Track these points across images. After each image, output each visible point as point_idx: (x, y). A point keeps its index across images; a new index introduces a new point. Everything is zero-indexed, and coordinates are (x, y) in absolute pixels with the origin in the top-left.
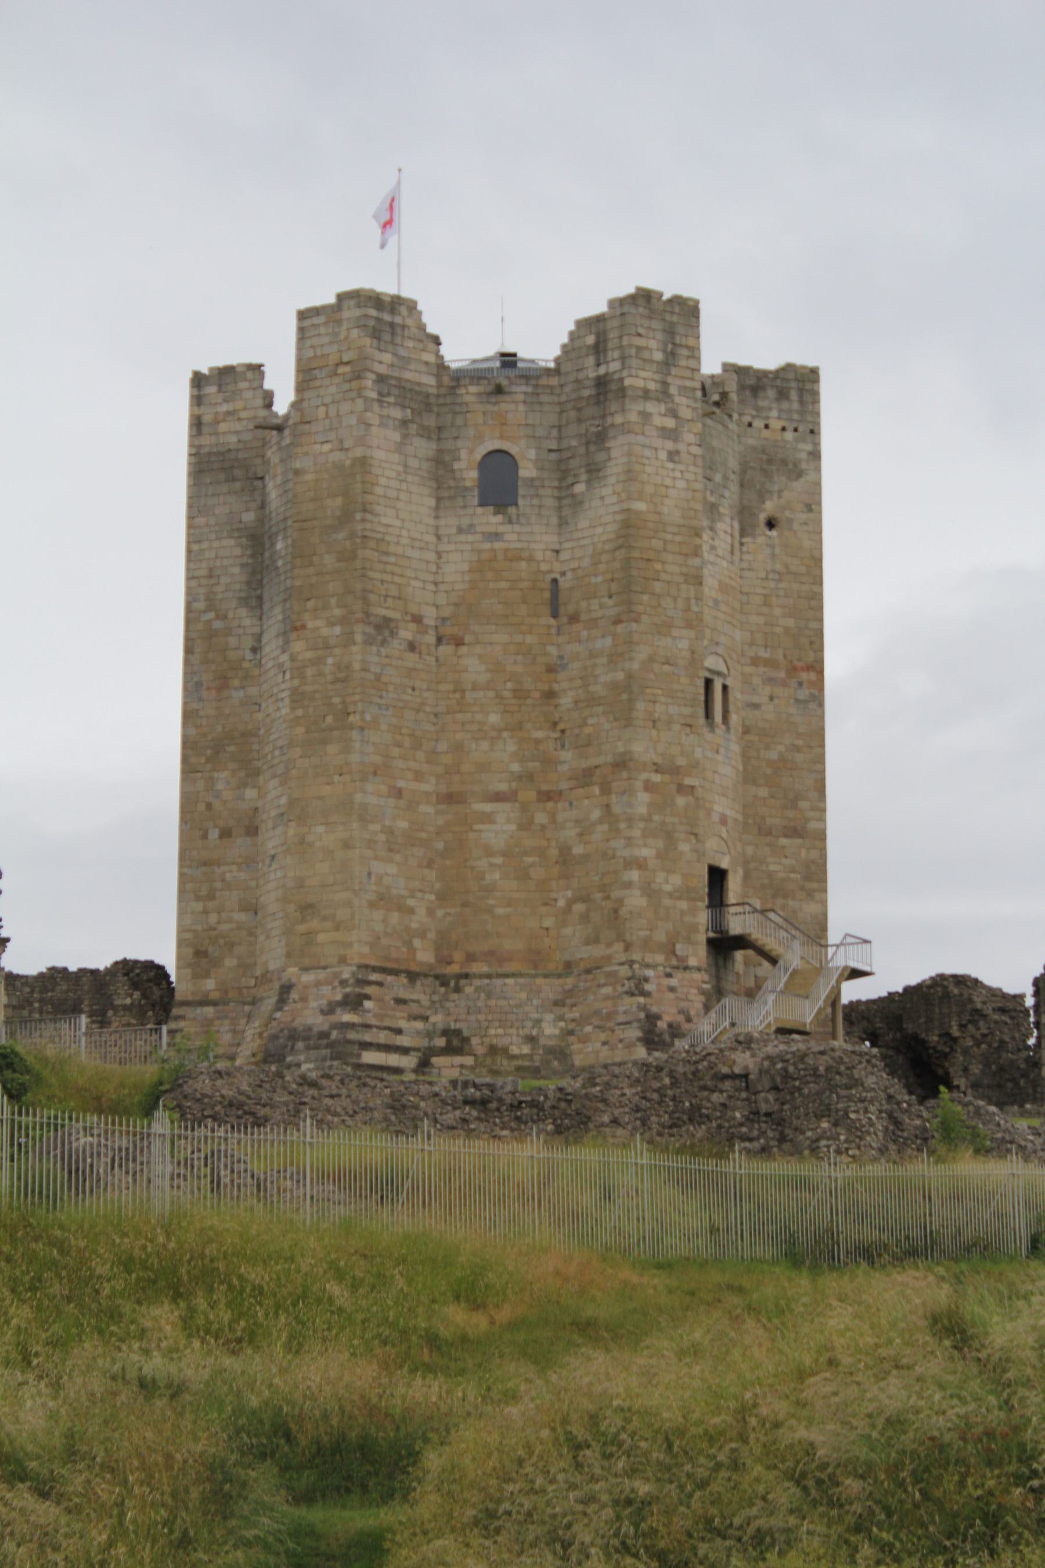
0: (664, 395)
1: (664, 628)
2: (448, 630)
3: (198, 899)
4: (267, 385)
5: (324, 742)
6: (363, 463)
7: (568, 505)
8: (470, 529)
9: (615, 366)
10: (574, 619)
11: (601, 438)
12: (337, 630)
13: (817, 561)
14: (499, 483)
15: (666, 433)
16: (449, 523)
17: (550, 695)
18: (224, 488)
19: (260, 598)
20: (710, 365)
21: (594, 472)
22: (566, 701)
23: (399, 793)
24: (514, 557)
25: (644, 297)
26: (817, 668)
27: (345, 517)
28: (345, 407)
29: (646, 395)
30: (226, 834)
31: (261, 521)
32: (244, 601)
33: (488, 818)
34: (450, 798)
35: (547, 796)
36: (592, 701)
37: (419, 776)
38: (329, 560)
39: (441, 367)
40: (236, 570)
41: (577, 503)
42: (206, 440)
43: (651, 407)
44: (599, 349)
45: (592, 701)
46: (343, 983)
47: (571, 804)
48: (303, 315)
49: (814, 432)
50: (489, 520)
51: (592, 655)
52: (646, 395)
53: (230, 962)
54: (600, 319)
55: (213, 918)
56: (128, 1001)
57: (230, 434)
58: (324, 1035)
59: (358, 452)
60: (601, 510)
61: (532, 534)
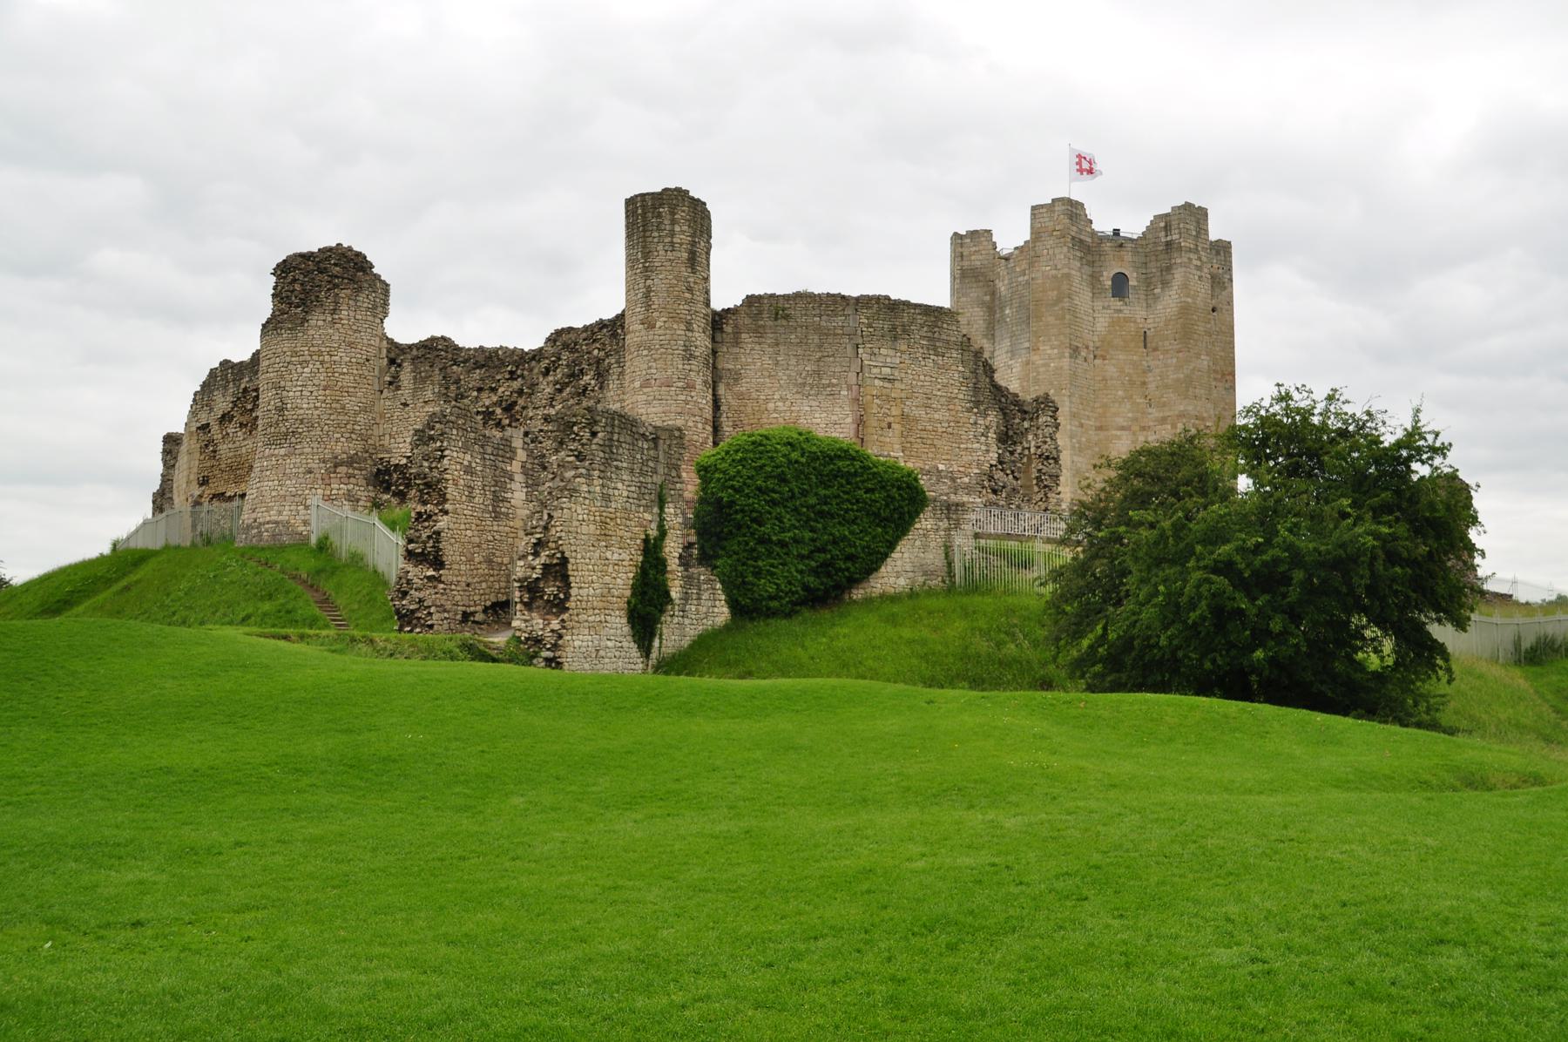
0: (1196, 251)
1: (1198, 356)
2: (1098, 353)
4: (1215, 233)
6: (1068, 276)
7: (1151, 299)
8: (1108, 307)
9: (1175, 237)
10: (1155, 349)
11: (1169, 269)
13: (1232, 328)
14: (1120, 285)
15: (1199, 268)
16: (1099, 304)
17: (1144, 383)
20: (1213, 235)
21: (1165, 284)
22: (1152, 386)
23: (1081, 425)
24: (1127, 320)
25: (1188, 206)
26: (1233, 374)
27: (1059, 300)
28: (1057, 251)
29: (1190, 250)
31: (993, 300)
32: (985, 336)
33: (1119, 438)
34: (1100, 428)
35: (1143, 429)
36: (1167, 386)
37: (1088, 418)
38: (1051, 320)
39: (1094, 233)
41: (1156, 298)
42: (966, 263)
43: (1192, 256)
44: (1167, 228)
45: (1167, 386)
48: (1034, 208)
49: (1230, 270)
50: (1117, 304)
51: (1166, 366)
52: (1190, 250)
54: (1167, 215)
57: (976, 260)
59: (1066, 270)
60: (1169, 302)
61: (1135, 310)
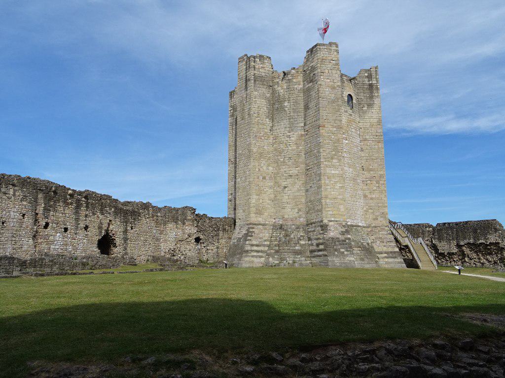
3: (257, 195)
5: (332, 158)
9: (373, 82)
12: (335, 129)
18: (262, 86)
19: (272, 117)
30: (264, 178)
40: (265, 108)
42: (256, 72)
46: (343, 226)
47: (367, 185)
53: (266, 214)
55: (261, 201)
56: (190, 218)
58: (343, 241)
